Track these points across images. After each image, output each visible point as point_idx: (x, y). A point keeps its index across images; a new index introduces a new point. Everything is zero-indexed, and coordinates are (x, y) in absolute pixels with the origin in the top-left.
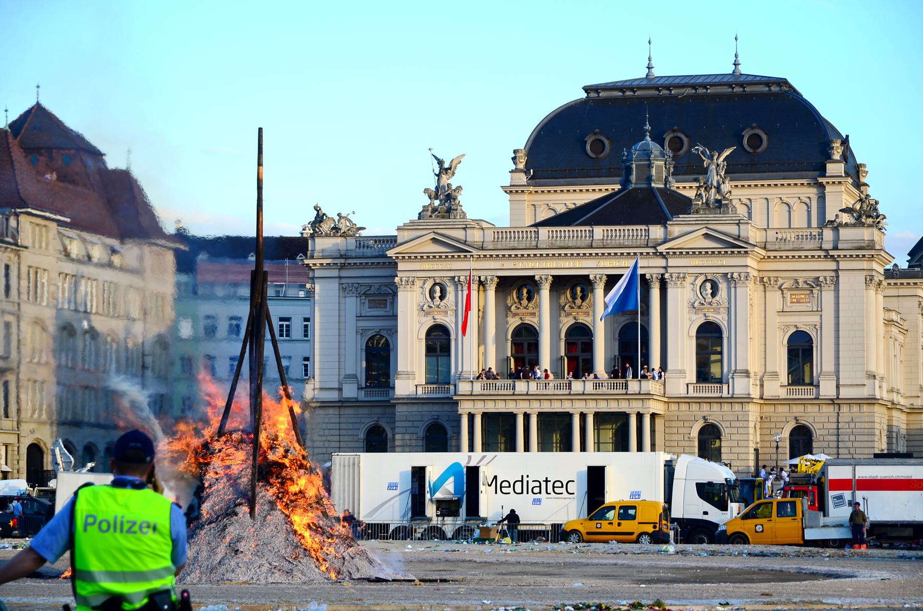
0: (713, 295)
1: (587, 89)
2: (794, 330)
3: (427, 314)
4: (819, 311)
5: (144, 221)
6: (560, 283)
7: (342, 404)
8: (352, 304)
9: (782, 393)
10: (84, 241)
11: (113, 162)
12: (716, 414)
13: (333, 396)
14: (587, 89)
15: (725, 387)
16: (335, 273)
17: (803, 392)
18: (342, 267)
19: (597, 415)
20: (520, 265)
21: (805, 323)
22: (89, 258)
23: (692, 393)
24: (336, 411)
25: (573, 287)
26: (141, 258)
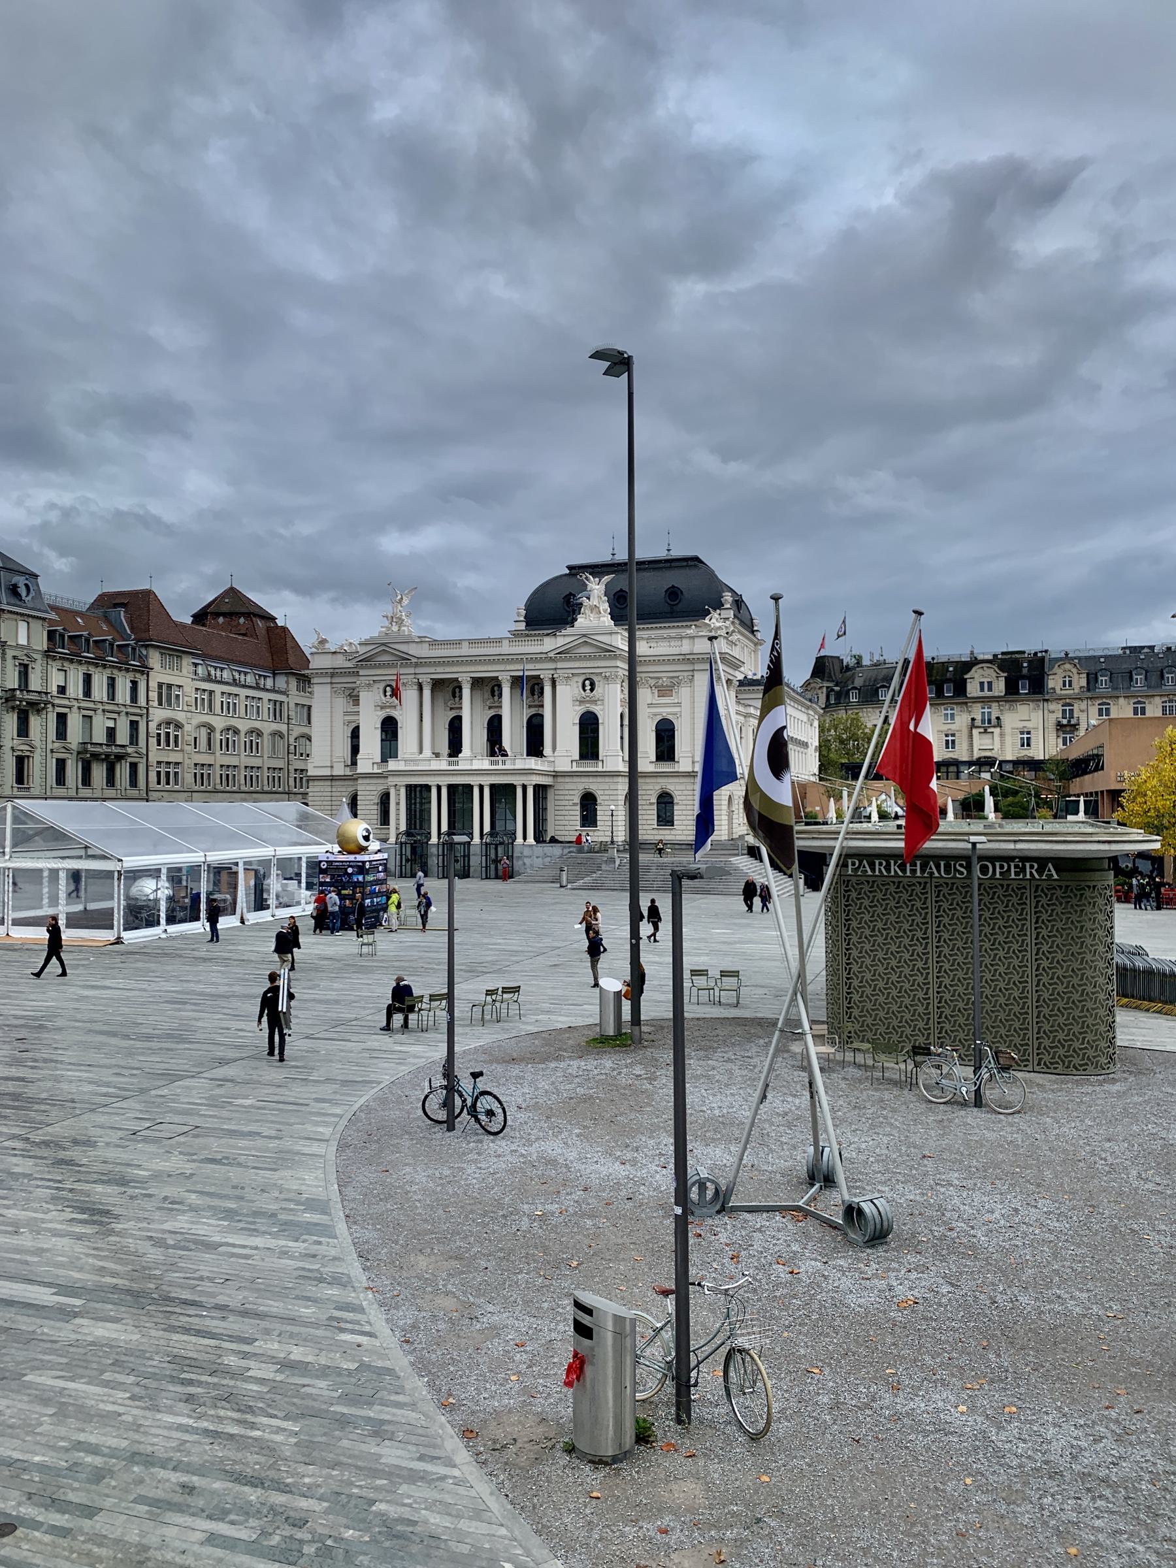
0: (592, 690)
1: (569, 567)
2: (659, 718)
3: (382, 708)
4: (679, 704)
5: (292, 660)
6: (477, 683)
7: (332, 778)
8: (341, 703)
9: (651, 768)
10: (232, 670)
11: (280, 623)
12: (594, 786)
13: (327, 772)
14: (569, 567)
15: (600, 764)
16: (329, 680)
17: (665, 767)
18: (332, 675)
19: (492, 786)
20: (448, 669)
21: (666, 712)
22: (234, 680)
23: (575, 769)
24: (329, 783)
25: (489, 687)
26: (287, 682)
